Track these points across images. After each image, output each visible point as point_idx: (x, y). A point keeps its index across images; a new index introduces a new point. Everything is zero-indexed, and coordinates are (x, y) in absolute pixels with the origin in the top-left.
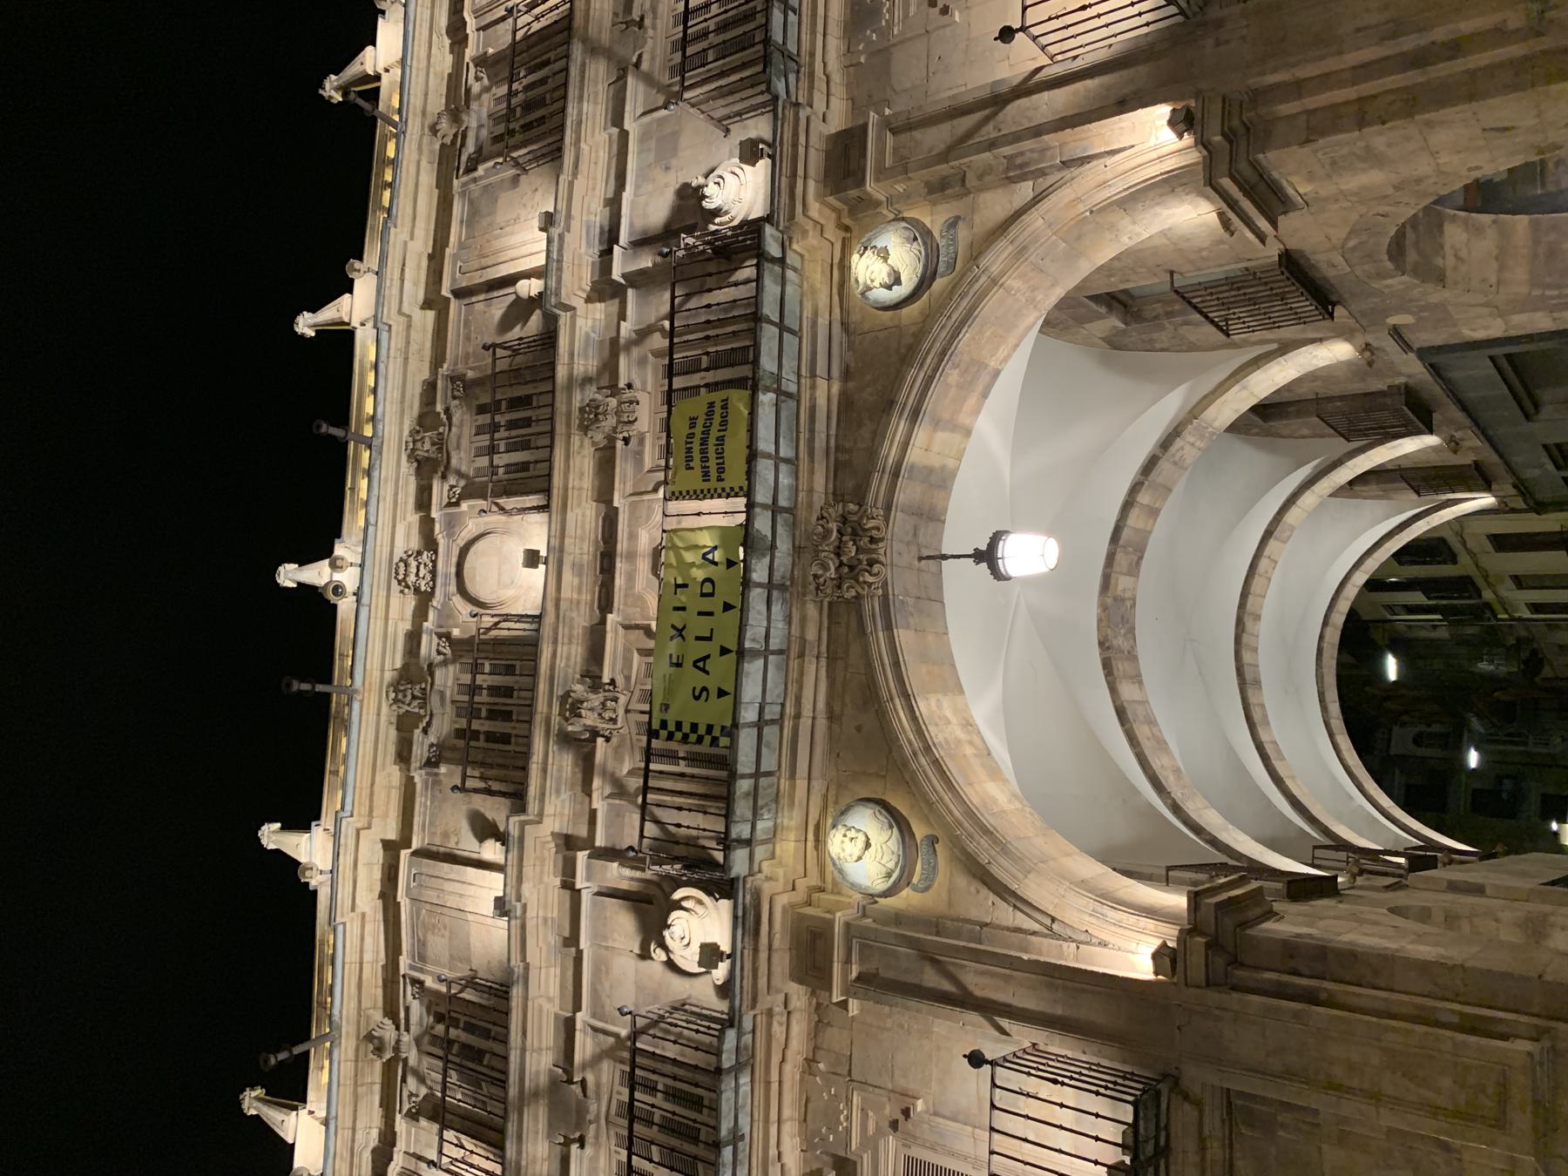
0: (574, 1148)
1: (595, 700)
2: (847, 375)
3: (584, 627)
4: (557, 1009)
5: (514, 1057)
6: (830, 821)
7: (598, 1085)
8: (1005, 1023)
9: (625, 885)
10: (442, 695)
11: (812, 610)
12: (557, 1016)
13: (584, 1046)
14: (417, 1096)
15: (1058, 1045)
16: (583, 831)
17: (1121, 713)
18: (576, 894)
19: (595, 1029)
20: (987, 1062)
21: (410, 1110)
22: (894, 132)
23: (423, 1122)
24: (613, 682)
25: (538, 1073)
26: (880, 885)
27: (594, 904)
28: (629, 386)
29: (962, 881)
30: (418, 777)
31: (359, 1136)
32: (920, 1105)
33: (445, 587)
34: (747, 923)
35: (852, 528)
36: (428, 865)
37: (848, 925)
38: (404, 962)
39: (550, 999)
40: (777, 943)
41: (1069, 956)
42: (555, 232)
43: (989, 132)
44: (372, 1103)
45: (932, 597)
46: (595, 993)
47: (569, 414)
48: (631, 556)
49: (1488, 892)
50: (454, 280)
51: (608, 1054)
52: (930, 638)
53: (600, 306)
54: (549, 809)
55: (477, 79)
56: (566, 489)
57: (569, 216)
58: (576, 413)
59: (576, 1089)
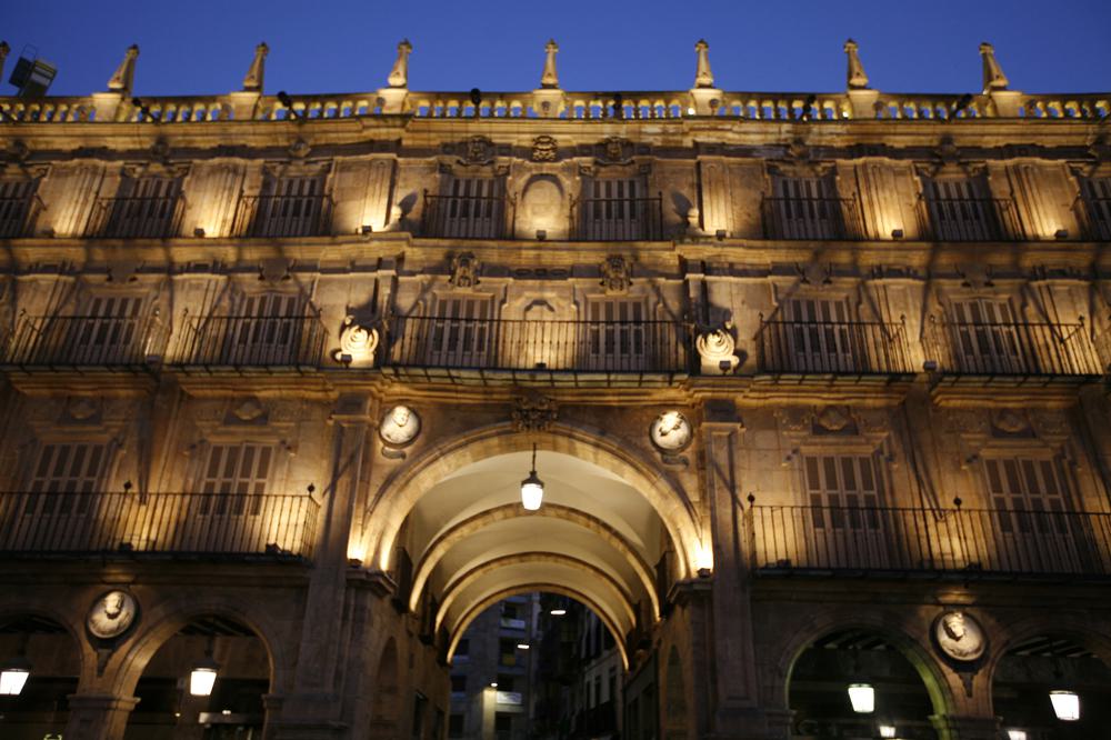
0: (257, 275)
1: (470, 274)
2: (622, 409)
6: (411, 405)
8: (328, 495)
9: (379, 298)
10: (477, 171)
11: (506, 397)
12: (317, 260)
13: (305, 277)
15: (322, 512)
16: (406, 267)
17: (487, 513)
19: (313, 283)
22: (729, 436)
23: (262, 177)
24: (478, 282)
27: (370, 279)
28: (631, 284)
29: (387, 471)
31: (251, 137)
32: (292, 454)
34: (364, 373)
35: (545, 416)
36: (388, 171)
37: (363, 422)
38: (339, 158)
39: (325, 255)
40: (355, 388)
41: (356, 522)
42: (715, 240)
45: (517, 447)
50: (706, 163)
51: (302, 290)
52: (497, 449)
53: (677, 262)
54: (415, 249)
55: (824, 168)
59: (285, 273)
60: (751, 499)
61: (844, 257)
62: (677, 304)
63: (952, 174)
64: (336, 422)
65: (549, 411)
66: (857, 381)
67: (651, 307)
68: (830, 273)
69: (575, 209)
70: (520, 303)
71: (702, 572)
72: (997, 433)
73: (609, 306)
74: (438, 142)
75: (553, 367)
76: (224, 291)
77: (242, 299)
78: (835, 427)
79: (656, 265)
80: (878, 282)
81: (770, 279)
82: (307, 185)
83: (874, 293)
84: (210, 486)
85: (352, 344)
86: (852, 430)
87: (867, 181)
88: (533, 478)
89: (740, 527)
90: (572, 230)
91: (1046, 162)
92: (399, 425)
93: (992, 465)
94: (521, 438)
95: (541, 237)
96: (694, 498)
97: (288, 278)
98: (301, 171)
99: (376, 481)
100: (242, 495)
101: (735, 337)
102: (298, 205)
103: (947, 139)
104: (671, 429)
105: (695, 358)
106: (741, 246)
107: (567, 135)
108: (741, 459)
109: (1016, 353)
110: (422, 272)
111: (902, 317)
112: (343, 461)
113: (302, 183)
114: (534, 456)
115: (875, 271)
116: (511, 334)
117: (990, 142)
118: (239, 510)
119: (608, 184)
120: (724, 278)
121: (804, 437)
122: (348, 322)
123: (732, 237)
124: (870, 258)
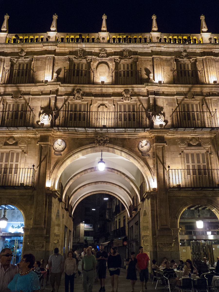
0: (11, 96)
1: (80, 96)
2: (129, 139)
3: (92, 92)
4: (31, 91)
5: (23, 85)
6: (63, 139)
7: (21, 100)
8: (38, 168)
9: (51, 104)
10: (81, 61)
11: (93, 135)
12: (30, 91)
13: (27, 97)
14: (14, 61)
15: (37, 173)
16: (59, 94)
17: (85, 170)
18: (49, 94)
19: (29, 99)
20: (33, 167)
21: (11, 59)
23: (10, 63)
25: (21, 89)
26: (54, 147)
27: (48, 97)
29: (56, 159)
30: (67, 56)
31: (6, 49)
32: (26, 155)
33: (99, 59)
35: (105, 142)
36: (52, 61)
37: (48, 144)
38: (35, 56)
40: (45, 134)
41: (48, 175)
42: (158, 84)
43: (159, 162)
44: (12, 50)
45: (96, 151)
46: (35, 98)
47: (127, 87)
48: (103, 100)
49: (63, 219)
50: (155, 58)
51: (26, 102)
52: (90, 152)
53: (146, 91)
54: (62, 88)
55: (193, 60)
56: (115, 87)
57: (161, 86)
58: (128, 89)
59: (20, 96)
60: (169, 167)
61: (198, 90)
62: (146, 105)
64: (40, 144)
65: (107, 140)
66: (201, 130)
67: (138, 106)
68: (194, 95)
69: (113, 73)
70: (96, 105)
71: (154, 189)
73: (125, 106)
74: (68, 50)
75: (108, 127)
78: (195, 144)
79: (140, 92)
80: (209, 97)
81: (175, 97)
82: (25, 65)
83: (207, 101)
85: (43, 119)
86: (199, 145)
87: (206, 64)
88: (101, 161)
89: (165, 175)
92: (59, 144)
94: (98, 148)
96: (152, 166)
97: (21, 97)
98: (23, 61)
99: (53, 162)
100: (11, 168)
101: (164, 116)
102: (23, 72)
104: (144, 145)
105: (152, 123)
106: (167, 86)
107: (111, 48)
108: (167, 155)
110: (64, 95)
111: (216, 110)
112: (43, 157)
113: (23, 65)
114: (102, 154)
115: (208, 94)
116: (93, 116)
118: (10, 172)
119: (124, 65)
120: (161, 97)
121: (185, 148)
122: (42, 112)
123: (163, 83)
124: (206, 90)
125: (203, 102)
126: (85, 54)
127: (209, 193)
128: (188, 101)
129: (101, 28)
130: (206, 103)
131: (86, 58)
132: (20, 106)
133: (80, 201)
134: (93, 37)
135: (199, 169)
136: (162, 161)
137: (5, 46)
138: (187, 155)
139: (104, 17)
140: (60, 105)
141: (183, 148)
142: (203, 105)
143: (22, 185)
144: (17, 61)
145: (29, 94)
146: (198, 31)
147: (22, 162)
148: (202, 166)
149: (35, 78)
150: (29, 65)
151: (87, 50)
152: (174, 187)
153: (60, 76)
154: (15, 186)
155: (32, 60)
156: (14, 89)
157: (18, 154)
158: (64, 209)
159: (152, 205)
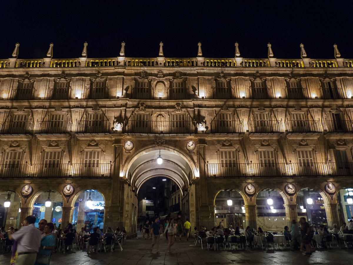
1: (143, 108)
2: (180, 141)
5: (101, 100)
7: (99, 111)
8: (114, 163)
9: (122, 115)
10: (144, 80)
12: (106, 105)
13: (103, 109)
16: (128, 106)
18: (121, 107)
19: (105, 110)
22: (204, 147)
26: (125, 147)
28: (182, 110)
29: (126, 156)
35: (162, 143)
36: (122, 80)
38: (109, 77)
41: (121, 168)
42: (202, 100)
43: (201, 158)
46: (109, 110)
47: (179, 102)
48: (160, 111)
50: (200, 78)
51: (103, 113)
55: (228, 79)
56: (169, 102)
57: (203, 101)
58: (179, 102)
59: (98, 108)
60: (208, 162)
62: (192, 115)
63: (258, 81)
65: (163, 142)
67: (187, 116)
68: (228, 107)
69: (168, 90)
70: (155, 115)
71: (197, 178)
72: (262, 145)
73: (177, 115)
74: (134, 72)
76: (84, 113)
77: (89, 115)
79: (188, 105)
80: (239, 109)
82: (101, 84)
83: (238, 112)
84: (86, 161)
86: (231, 145)
87: (238, 82)
88: (160, 156)
89: (206, 168)
90: (167, 97)
91: (280, 77)
92: (128, 145)
93: (261, 152)
94: (157, 148)
95: (160, 98)
96: (196, 161)
97: (99, 109)
98: (100, 80)
100: (94, 164)
101: (206, 124)
103: (257, 72)
104: (191, 145)
105: (196, 129)
106: (208, 101)
107: (166, 70)
109: (268, 126)
110: (132, 108)
111: (243, 119)
112: (117, 155)
113: (100, 83)
116: (154, 124)
117: (267, 72)
118: (93, 166)
119: (176, 84)
120: (203, 109)
121: (220, 147)
123: (206, 98)
124: (237, 103)
125: (235, 113)
126: (147, 75)
127: (237, 181)
128: (223, 111)
129: (159, 53)
130: (237, 113)
131: (147, 78)
132: (99, 116)
133: (143, 183)
134: (153, 61)
135: (230, 164)
136: (203, 157)
137: (86, 69)
138: (222, 152)
139: (161, 44)
140: (128, 115)
141: (219, 147)
142: (234, 114)
143: (103, 175)
144: (95, 80)
145: (105, 107)
146: (234, 56)
147: (102, 158)
148: (232, 160)
149: (109, 93)
150: (104, 83)
151: (149, 72)
152: (211, 177)
153: (128, 92)
154: (98, 177)
155: (106, 80)
156: (94, 103)
157: (98, 153)
158: (132, 191)
159: (196, 189)
